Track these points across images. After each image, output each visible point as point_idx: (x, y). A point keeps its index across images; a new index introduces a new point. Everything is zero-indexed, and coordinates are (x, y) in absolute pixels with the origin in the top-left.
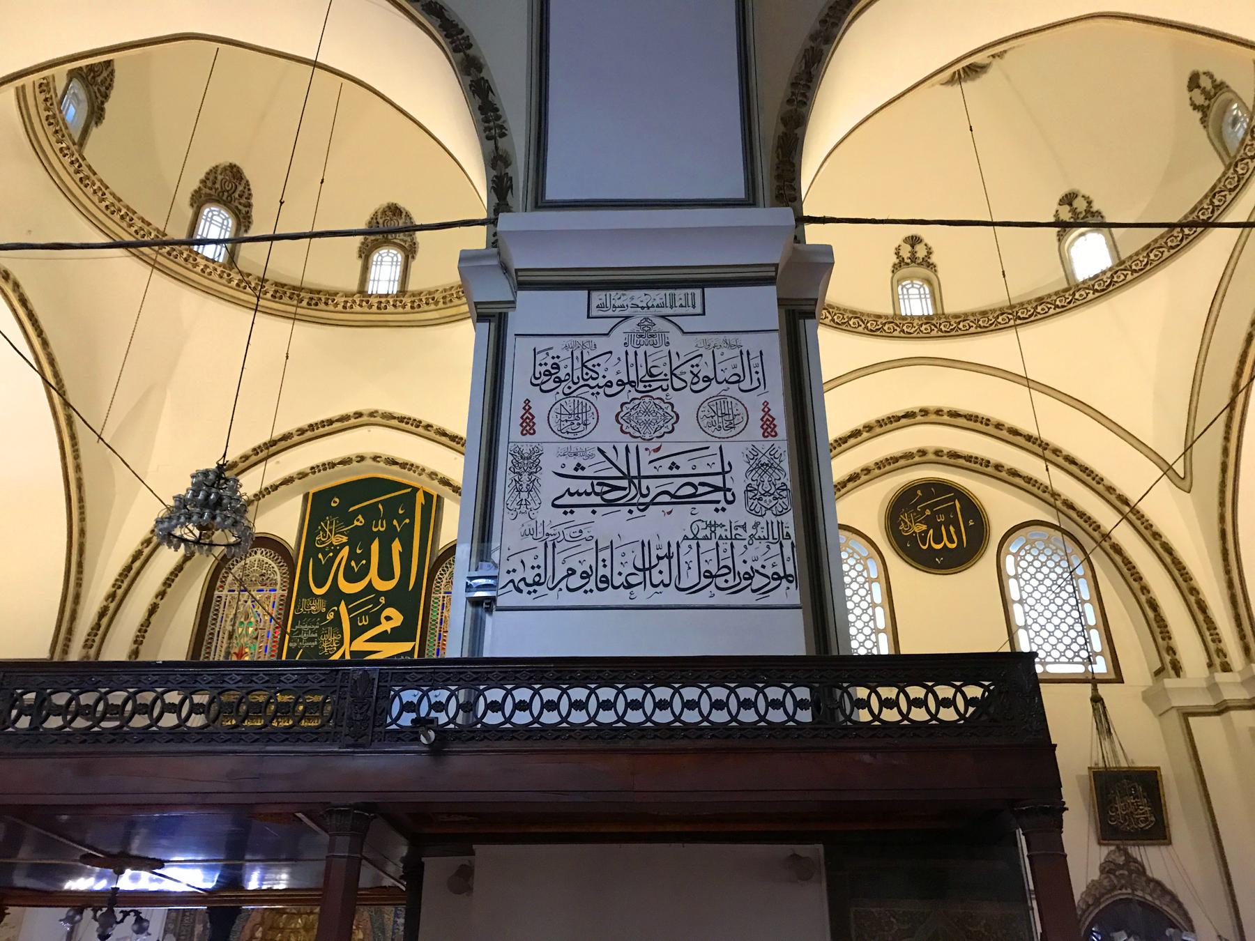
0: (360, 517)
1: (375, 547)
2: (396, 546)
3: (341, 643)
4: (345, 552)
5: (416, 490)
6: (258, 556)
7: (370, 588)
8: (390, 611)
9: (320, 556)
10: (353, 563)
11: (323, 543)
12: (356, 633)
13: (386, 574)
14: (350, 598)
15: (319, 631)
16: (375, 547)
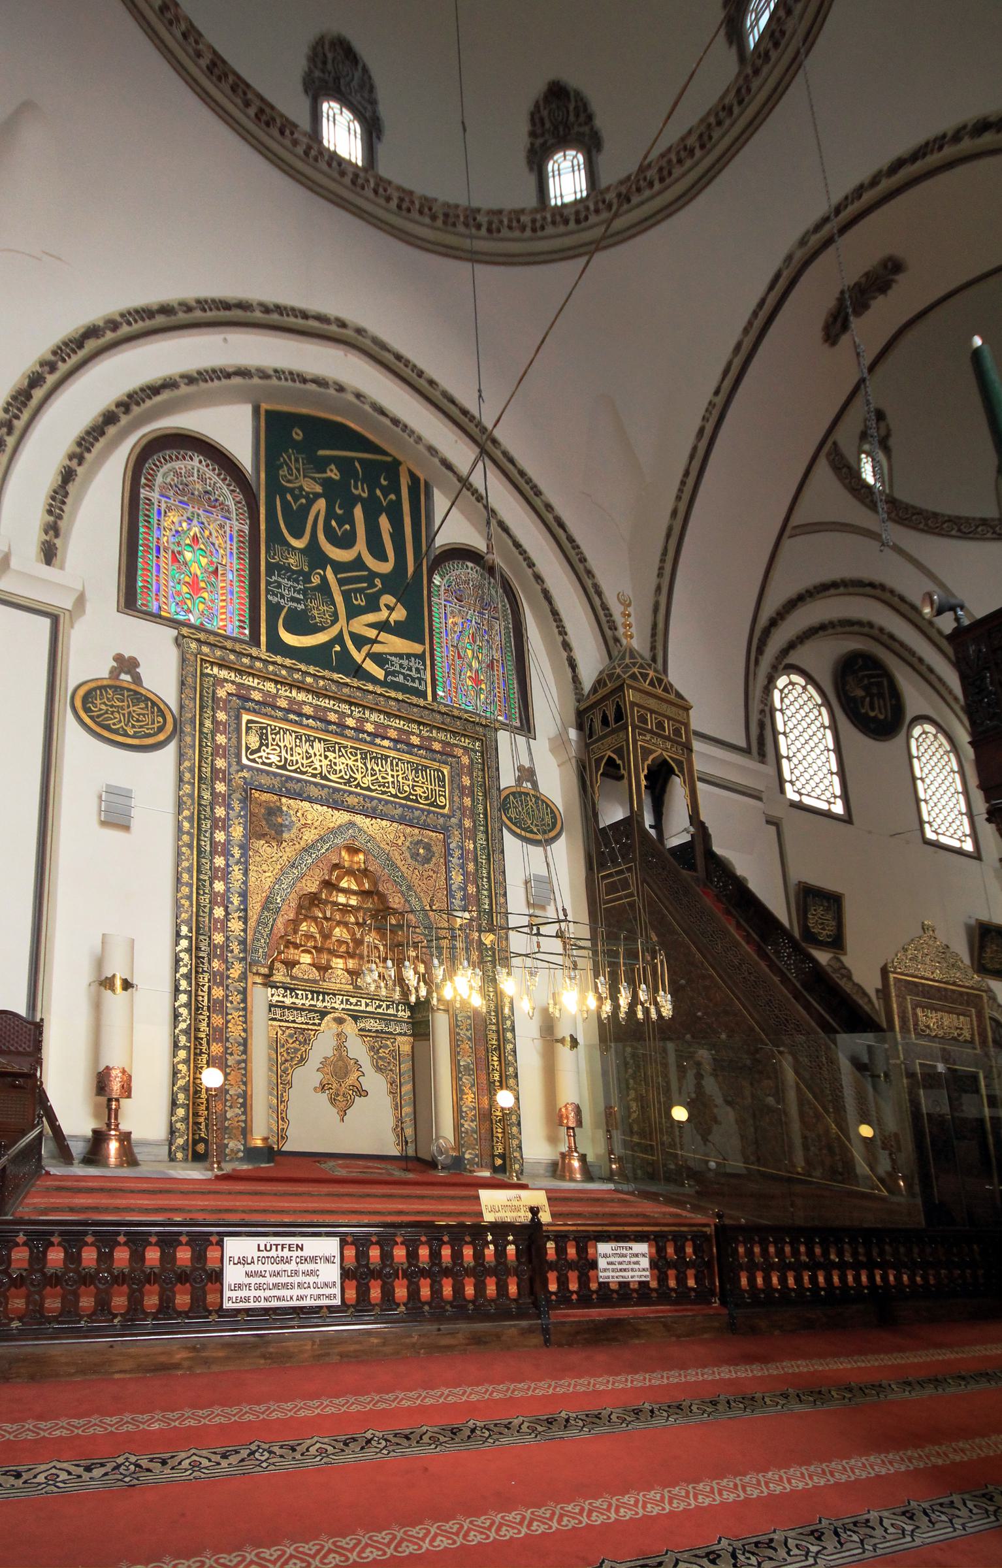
0: (333, 467)
1: (358, 512)
2: (384, 523)
4: (321, 504)
5: (397, 463)
6: (196, 463)
7: (358, 563)
8: (388, 599)
9: (289, 497)
12: (353, 612)
14: (338, 567)
16: (358, 512)
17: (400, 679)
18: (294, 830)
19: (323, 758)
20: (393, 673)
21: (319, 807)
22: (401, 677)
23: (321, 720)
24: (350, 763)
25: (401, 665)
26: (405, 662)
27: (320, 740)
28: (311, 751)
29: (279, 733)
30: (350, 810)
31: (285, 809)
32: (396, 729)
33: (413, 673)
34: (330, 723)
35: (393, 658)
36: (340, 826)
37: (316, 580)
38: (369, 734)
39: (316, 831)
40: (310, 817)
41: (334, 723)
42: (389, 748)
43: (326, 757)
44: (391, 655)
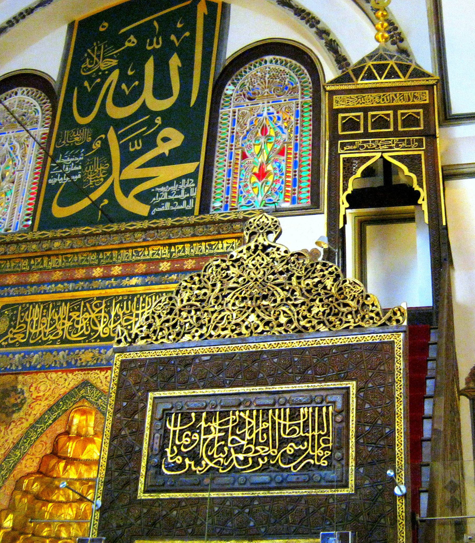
3: (109, 172)
10: (124, 86)
11: (90, 69)
13: (162, 90)
14: (118, 124)
15: (83, 164)
17: (167, 207)
18: (25, 407)
19: (66, 321)
20: (159, 205)
21: (54, 375)
22: (168, 204)
23: (69, 281)
24: (93, 316)
25: (170, 193)
26: (174, 188)
27: (66, 301)
28: (56, 317)
29: (28, 309)
30: (85, 368)
31: (19, 387)
32: (144, 261)
33: (183, 196)
34: (76, 281)
35: (157, 189)
36: (73, 389)
37: (97, 145)
38: (116, 277)
39: (47, 402)
40: (42, 388)
41: (81, 280)
42: (136, 285)
43: (70, 318)
44: (159, 186)
